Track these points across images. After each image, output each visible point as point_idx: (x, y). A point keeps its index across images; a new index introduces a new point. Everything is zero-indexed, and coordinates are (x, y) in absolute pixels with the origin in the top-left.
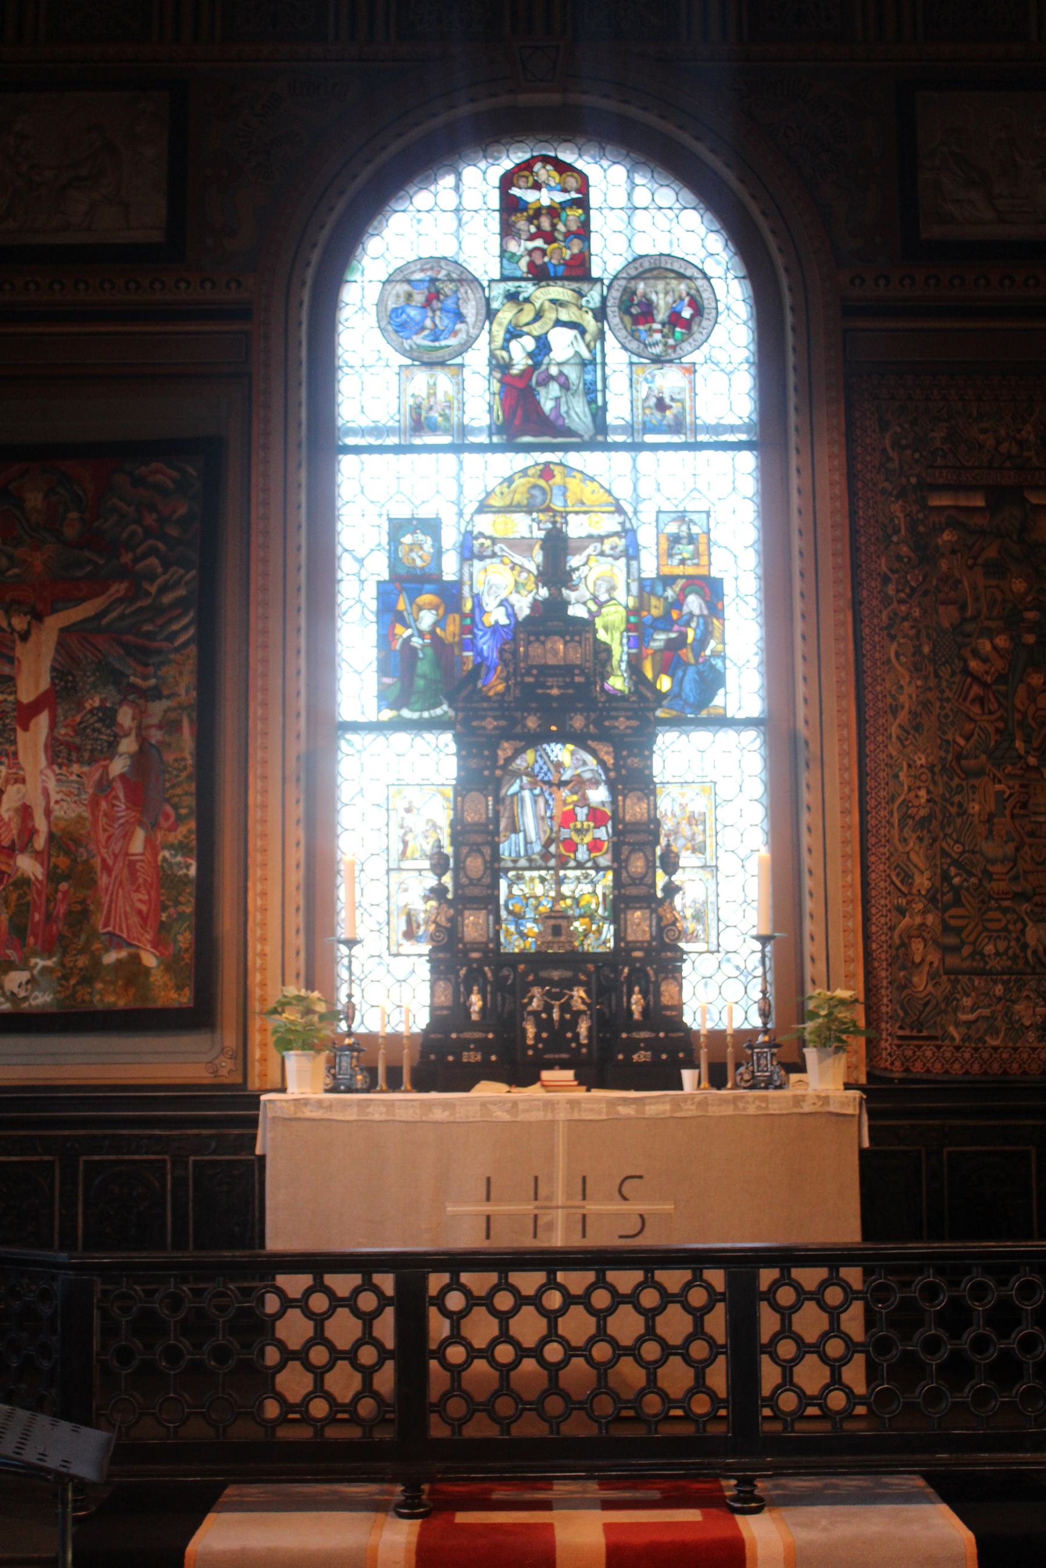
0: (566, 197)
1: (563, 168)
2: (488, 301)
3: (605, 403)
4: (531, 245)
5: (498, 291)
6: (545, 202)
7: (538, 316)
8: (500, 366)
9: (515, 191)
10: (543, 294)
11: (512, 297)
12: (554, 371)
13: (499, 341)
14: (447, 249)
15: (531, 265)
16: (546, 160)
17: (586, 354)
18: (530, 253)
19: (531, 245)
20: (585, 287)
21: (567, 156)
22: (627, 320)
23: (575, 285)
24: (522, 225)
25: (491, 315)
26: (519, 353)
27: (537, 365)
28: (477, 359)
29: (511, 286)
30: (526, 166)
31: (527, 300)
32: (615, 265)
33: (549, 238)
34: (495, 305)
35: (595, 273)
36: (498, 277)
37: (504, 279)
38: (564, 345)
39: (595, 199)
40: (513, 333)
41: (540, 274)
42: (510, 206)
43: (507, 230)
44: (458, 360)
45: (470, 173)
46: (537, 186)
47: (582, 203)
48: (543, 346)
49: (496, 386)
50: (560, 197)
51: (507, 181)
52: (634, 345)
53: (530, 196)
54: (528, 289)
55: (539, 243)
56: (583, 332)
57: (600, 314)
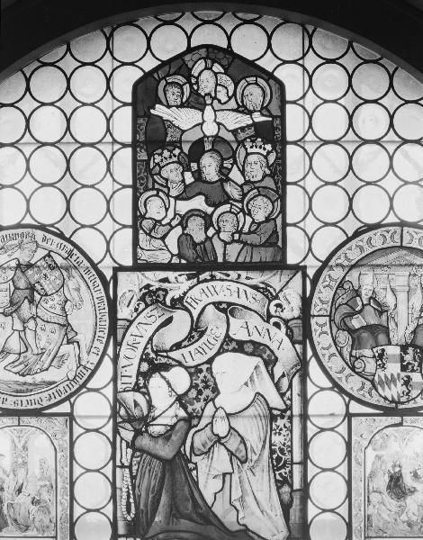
0: (245, 120)
1: (240, 68)
2: (113, 305)
3: (306, 485)
4: (184, 207)
5: (130, 285)
6: (210, 129)
7: (197, 330)
8: (131, 420)
9: (159, 110)
10: (205, 293)
11: (151, 297)
12: (221, 428)
13: (130, 371)
14: (48, 209)
15: (185, 238)
16: (213, 54)
17: (276, 401)
18: (184, 220)
19: (184, 207)
20: (275, 280)
21: (248, 42)
22: (343, 337)
23: (257, 278)
24: (172, 172)
25: (115, 330)
26: (162, 393)
27: (190, 420)
28: (93, 407)
29: (152, 278)
30: (178, 66)
31: (178, 303)
32: (326, 242)
33: (218, 197)
34: (124, 312)
35: (292, 259)
36: (128, 262)
37: (139, 267)
38: (237, 379)
39: (295, 124)
40: (155, 364)
41: (199, 263)
42: (151, 138)
43: (144, 180)
44: (65, 408)
45: (88, 83)
46: (196, 101)
47: (271, 133)
48: (203, 384)
49: (125, 455)
50: (234, 121)
51: (145, 93)
52: (353, 384)
53: (185, 119)
54: (179, 284)
55: (199, 203)
56: (270, 362)
57: (302, 332)
